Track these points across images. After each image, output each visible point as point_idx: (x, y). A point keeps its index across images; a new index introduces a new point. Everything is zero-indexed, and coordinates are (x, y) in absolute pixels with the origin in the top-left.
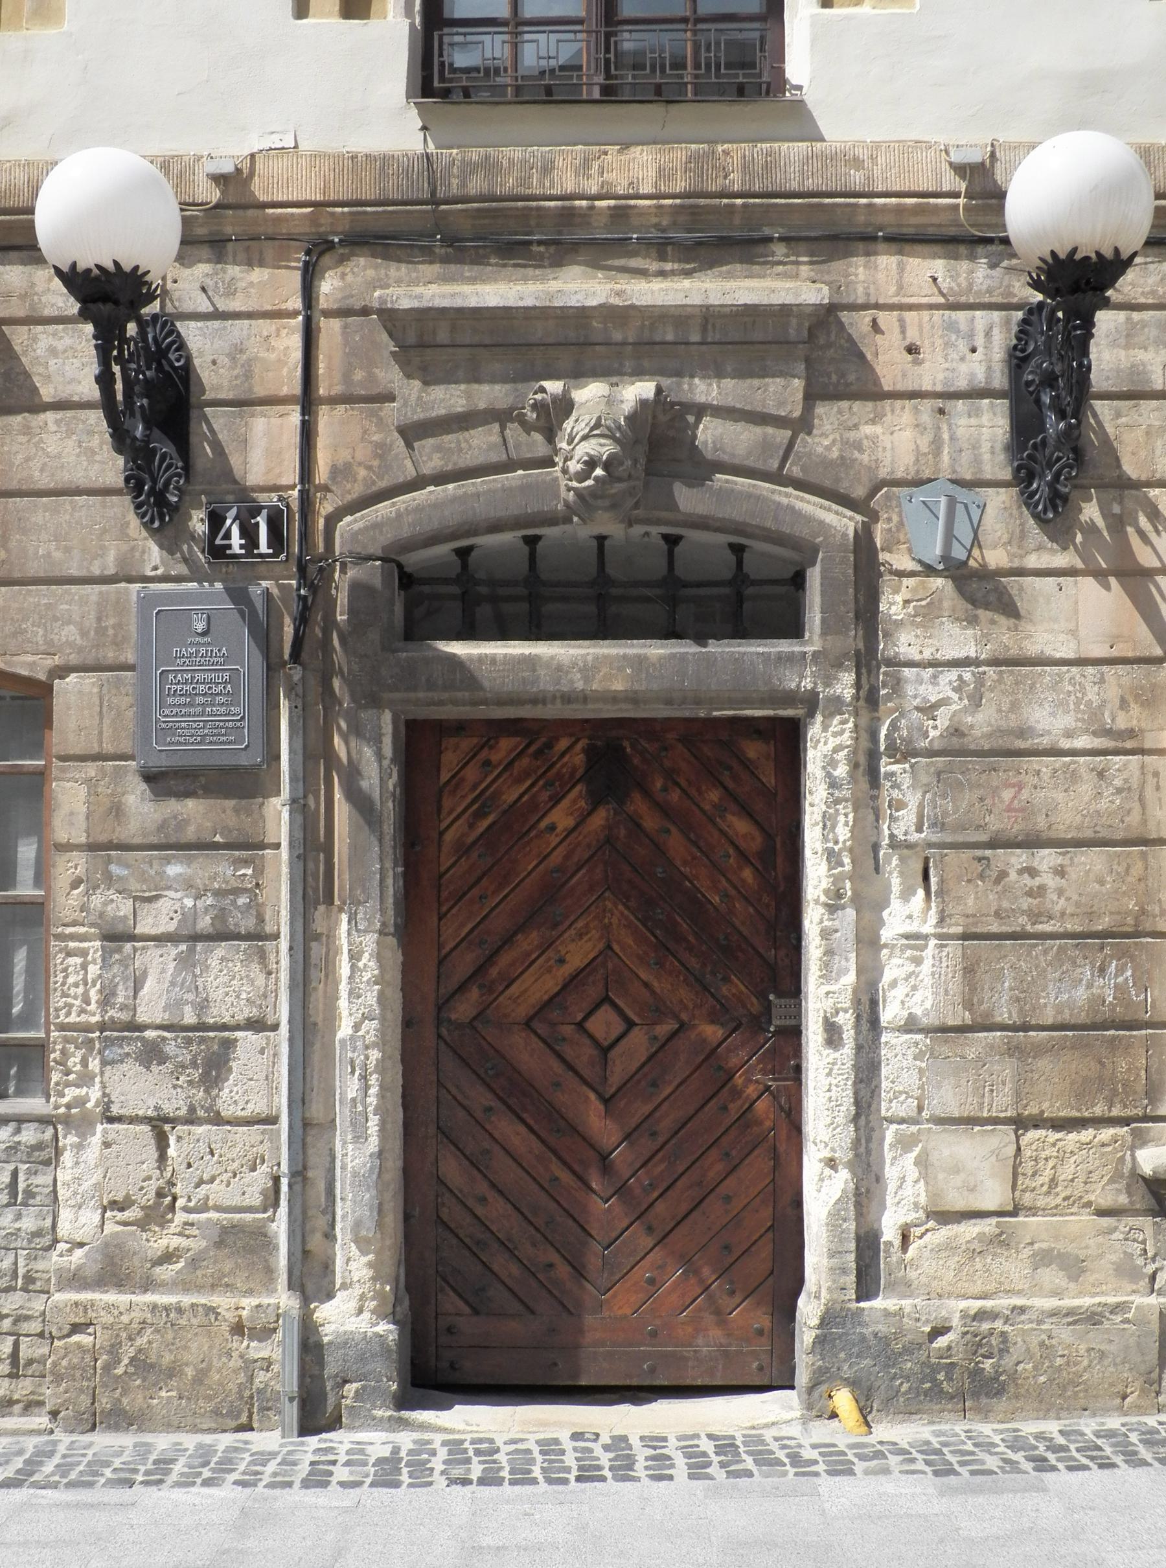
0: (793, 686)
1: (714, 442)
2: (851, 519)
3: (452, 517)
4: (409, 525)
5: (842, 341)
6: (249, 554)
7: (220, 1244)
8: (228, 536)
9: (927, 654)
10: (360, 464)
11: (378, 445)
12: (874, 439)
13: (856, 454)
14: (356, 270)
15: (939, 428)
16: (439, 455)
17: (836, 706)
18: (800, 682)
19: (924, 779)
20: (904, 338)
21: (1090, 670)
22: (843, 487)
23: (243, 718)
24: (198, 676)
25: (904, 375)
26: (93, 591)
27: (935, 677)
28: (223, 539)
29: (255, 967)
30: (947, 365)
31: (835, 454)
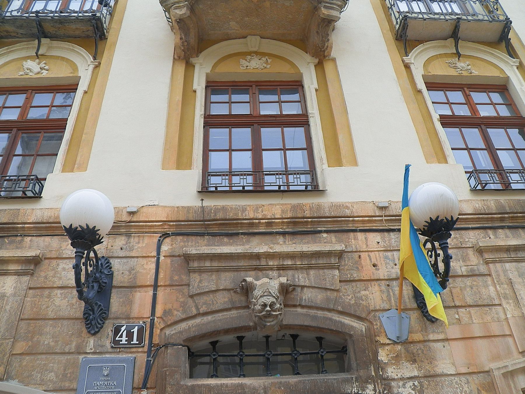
0: (349, 391)
1: (308, 299)
2: (363, 325)
3: (210, 328)
4: (193, 331)
5: (350, 264)
6: (129, 343)
8: (121, 336)
9: (399, 376)
10: (175, 309)
11: (182, 302)
12: (366, 296)
13: (361, 302)
14: (177, 243)
15: (389, 291)
16: (205, 306)
18: (352, 390)
20: (371, 262)
21: (463, 379)
22: (358, 313)
26: (63, 358)
27: (404, 385)
31: (353, 302)
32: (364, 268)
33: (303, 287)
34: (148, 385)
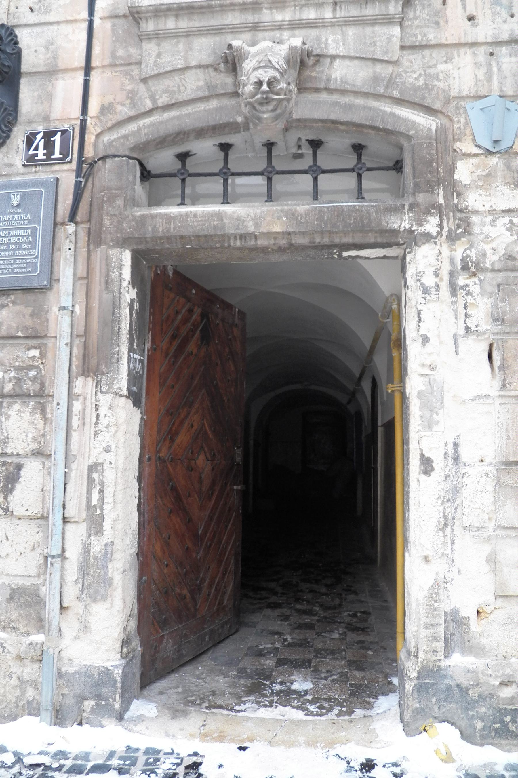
0: (396, 226)
1: (341, 79)
2: (433, 121)
3: (172, 128)
4: (145, 134)
5: (424, 16)
7: (10, 599)
8: (36, 149)
9: (487, 207)
10: (118, 103)
13: (436, 82)
15: (490, 64)
16: (166, 95)
17: (428, 237)
18: (401, 224)
19: (489, 289)
20: (465, 11)
22: (427, 102)
23: (37, 257)
24: (13, 232)
25: (466, 34)
28: (34, 150)
29: (38, 416)
30: (494, 26)
32: (450, 24)
33: (334, 57)
34: (78, 219)
